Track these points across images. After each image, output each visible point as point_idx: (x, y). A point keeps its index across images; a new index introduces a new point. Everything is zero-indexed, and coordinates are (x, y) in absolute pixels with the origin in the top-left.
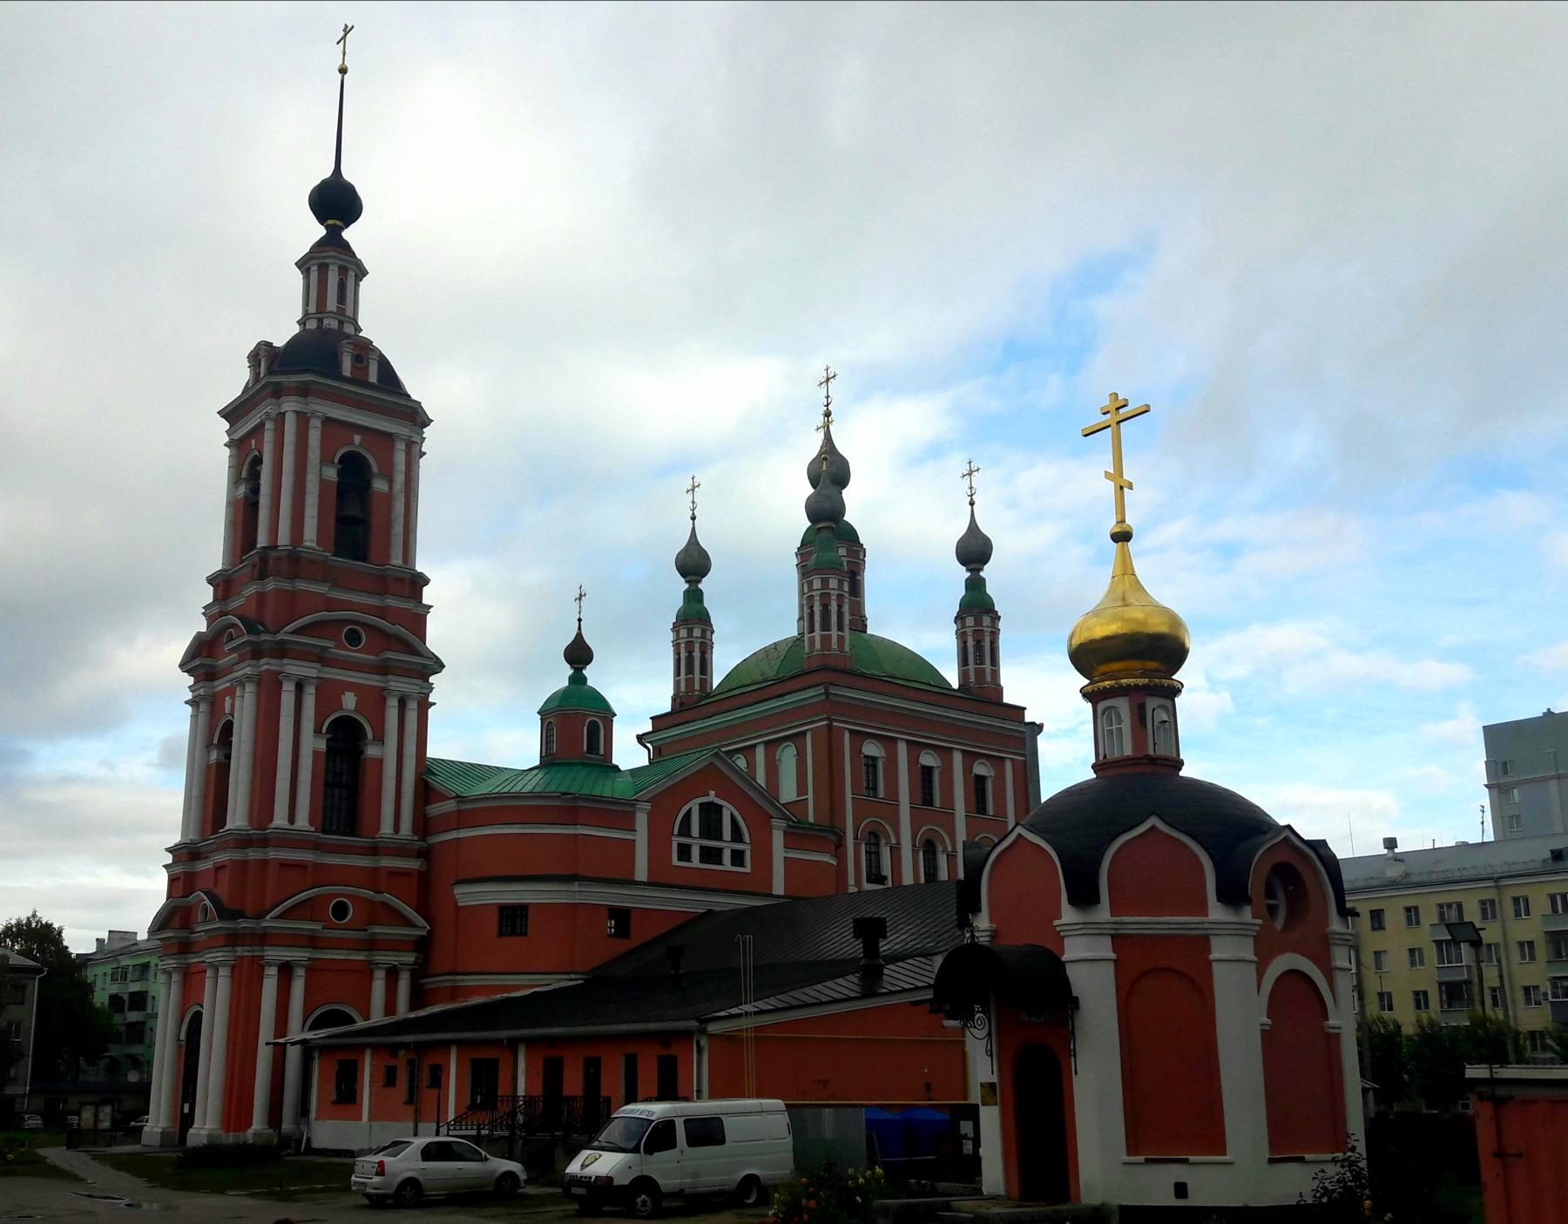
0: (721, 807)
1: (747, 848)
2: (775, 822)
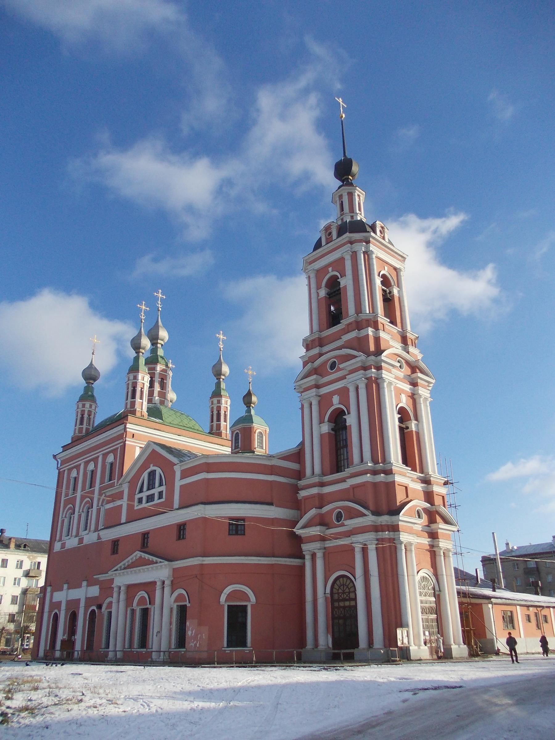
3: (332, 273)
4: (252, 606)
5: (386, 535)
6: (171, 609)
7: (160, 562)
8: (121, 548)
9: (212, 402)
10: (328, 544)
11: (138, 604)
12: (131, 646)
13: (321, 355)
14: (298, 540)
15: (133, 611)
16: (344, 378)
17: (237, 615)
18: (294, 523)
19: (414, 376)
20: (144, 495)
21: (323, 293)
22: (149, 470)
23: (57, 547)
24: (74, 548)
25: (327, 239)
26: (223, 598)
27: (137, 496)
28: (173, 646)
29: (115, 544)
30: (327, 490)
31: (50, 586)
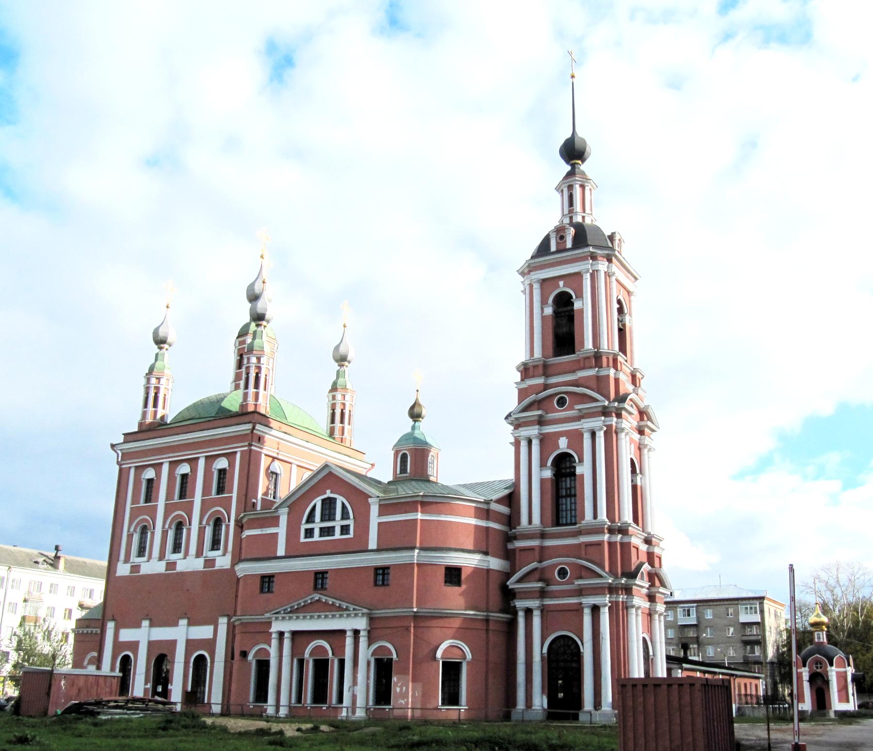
0: (335, 499)
1: (350, 522)
2: (370, 500)
3: (562, 286)
4: (468, 663)
5: (622, 598)
6: (369, 663)
7: (354, 609)
8: (275, 587)
9: (334, 398)
10: (548, 602)
11: (311, 654)
12: (299, 700)
13: (546, 387)
14: (508, 595)
15: (301, 662)
16: (579, 418)
17: (452, 670)
18: (508, 575)
19: (642, 423)
20: (317, 525)
21: (549, 311)
22: (325, 496)
23: (123, 570)
24: (159, 575)
25: (557, 243)
26: (439, 654)
27: (304, 527)
28: (371, 703)
29: (267, 581)
30: (549, 543)
31: (113, 619)
